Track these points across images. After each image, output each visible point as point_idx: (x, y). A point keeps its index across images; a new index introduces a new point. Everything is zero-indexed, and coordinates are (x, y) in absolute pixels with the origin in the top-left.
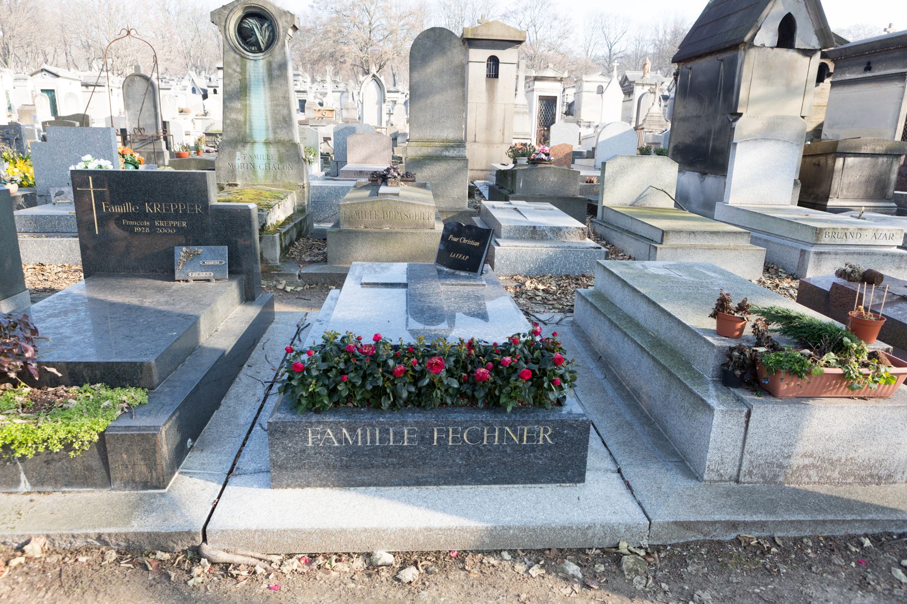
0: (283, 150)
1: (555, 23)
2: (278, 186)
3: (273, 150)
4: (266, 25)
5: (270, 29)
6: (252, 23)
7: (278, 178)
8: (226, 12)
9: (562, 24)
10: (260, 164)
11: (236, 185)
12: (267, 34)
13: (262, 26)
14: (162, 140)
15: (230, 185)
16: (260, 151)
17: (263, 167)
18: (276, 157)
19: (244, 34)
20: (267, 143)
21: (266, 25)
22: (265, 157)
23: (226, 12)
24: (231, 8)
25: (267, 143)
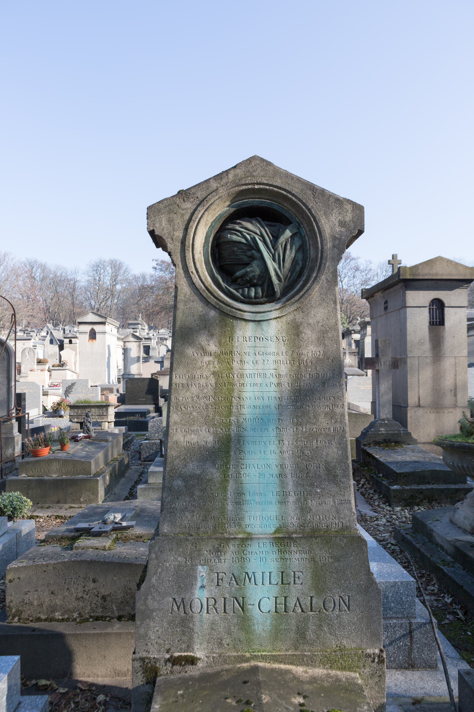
0: (323, 555)
1: (358, 274)
2: (309, 661)
3: (297, 559)
4: (288, 233)
5: (298, 242)
6: (251, 229)
7: (310, 635)
8: (189, 206)
9: (363, 274)
10: (262, 598)
11: (192, 661)
12: (290, 255)
13: (276, 238)
14: (14, 421)
15: (175, 661)
16: (263, 562)
17: (268, 605)
18: (305, 578)
19: (229, 259)
20: (283, 539)
21: (288, 233)
22: (276, 579)
23: (189, 206)
24: (200, 194)
25: (283, 539)
